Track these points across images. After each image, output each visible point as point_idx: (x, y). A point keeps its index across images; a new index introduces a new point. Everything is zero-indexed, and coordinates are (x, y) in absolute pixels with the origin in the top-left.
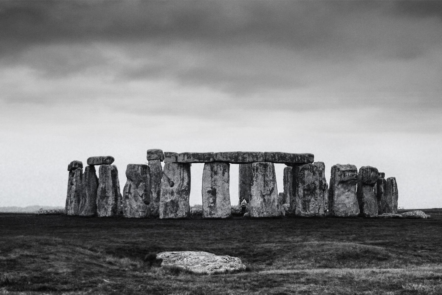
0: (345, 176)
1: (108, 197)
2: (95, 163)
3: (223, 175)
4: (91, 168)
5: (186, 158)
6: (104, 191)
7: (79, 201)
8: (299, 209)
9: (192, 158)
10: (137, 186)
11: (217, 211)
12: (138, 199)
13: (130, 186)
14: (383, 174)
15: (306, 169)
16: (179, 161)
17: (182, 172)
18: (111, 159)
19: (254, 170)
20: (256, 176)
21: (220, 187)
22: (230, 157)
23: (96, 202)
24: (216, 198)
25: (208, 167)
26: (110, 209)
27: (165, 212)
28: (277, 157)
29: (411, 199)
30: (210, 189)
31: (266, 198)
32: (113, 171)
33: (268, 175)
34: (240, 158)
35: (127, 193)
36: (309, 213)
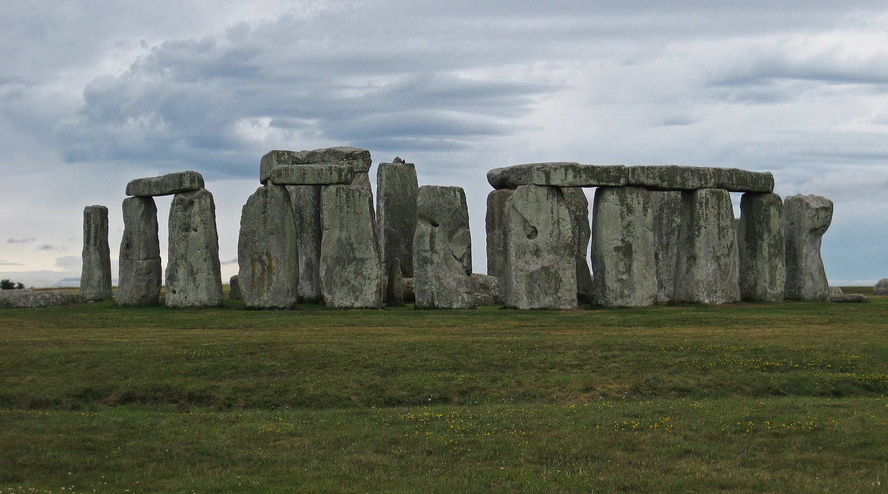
1: (363, 261)
3: (645, 215)
9: (584, 176)
13: (432, 236)
16: (553, 183)
17: (555, 207)
19: (701, 206)
21: (640, 241)
22: (661, 177)
24: (631, 261)
27: (530, 293)
28: (734, 181)
29: (844, 263)
30: (620, 244)
31: (723, 261)
34: (679, 179)
35: (425, 251)
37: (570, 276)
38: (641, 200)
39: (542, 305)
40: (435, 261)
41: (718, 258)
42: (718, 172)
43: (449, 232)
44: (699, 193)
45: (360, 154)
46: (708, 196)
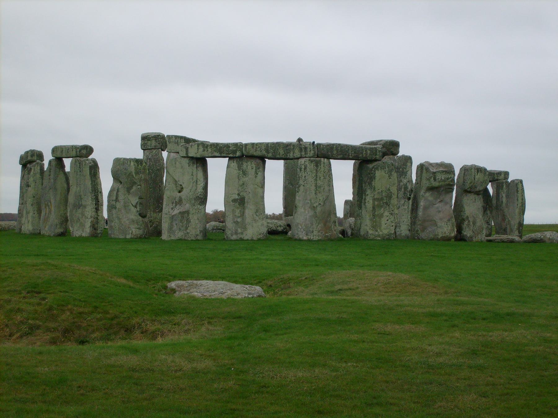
0: (435, 179)
1: (85, 207)
2: (64, 155)
3: (256, 177)
4: (58, 161)
5: (201, 149)
6: (79, 197)
7: (39, 211)
8: (366, 227)
9: (210, 150)
10: (129, 190)
11: (245, 228)
12: (130, 210)
13: (118, 191)
14: (507, 174)
15: (377, 169)
16: (190, 155)
18: (89, 150)
19: (301, 170)
20: (303, 177)
21: (250, 195)
23: (66, 214)
24: (244, 208)
25: (234, 164)
26: (88, 224)
27: (170, 229)
28: (335, 152)
30: (237, 197)
32: (91, 168)
33: (322, 178)
36: (381, 233)
37: (196, 218)
38: (254, 166)
39: (177, 238)
40: (118, 207)
41: (314, 207)
42: (319, 146)
43: (127, 188)
44: (300, 160)
45: (152, 137)
46: (307, 163)
